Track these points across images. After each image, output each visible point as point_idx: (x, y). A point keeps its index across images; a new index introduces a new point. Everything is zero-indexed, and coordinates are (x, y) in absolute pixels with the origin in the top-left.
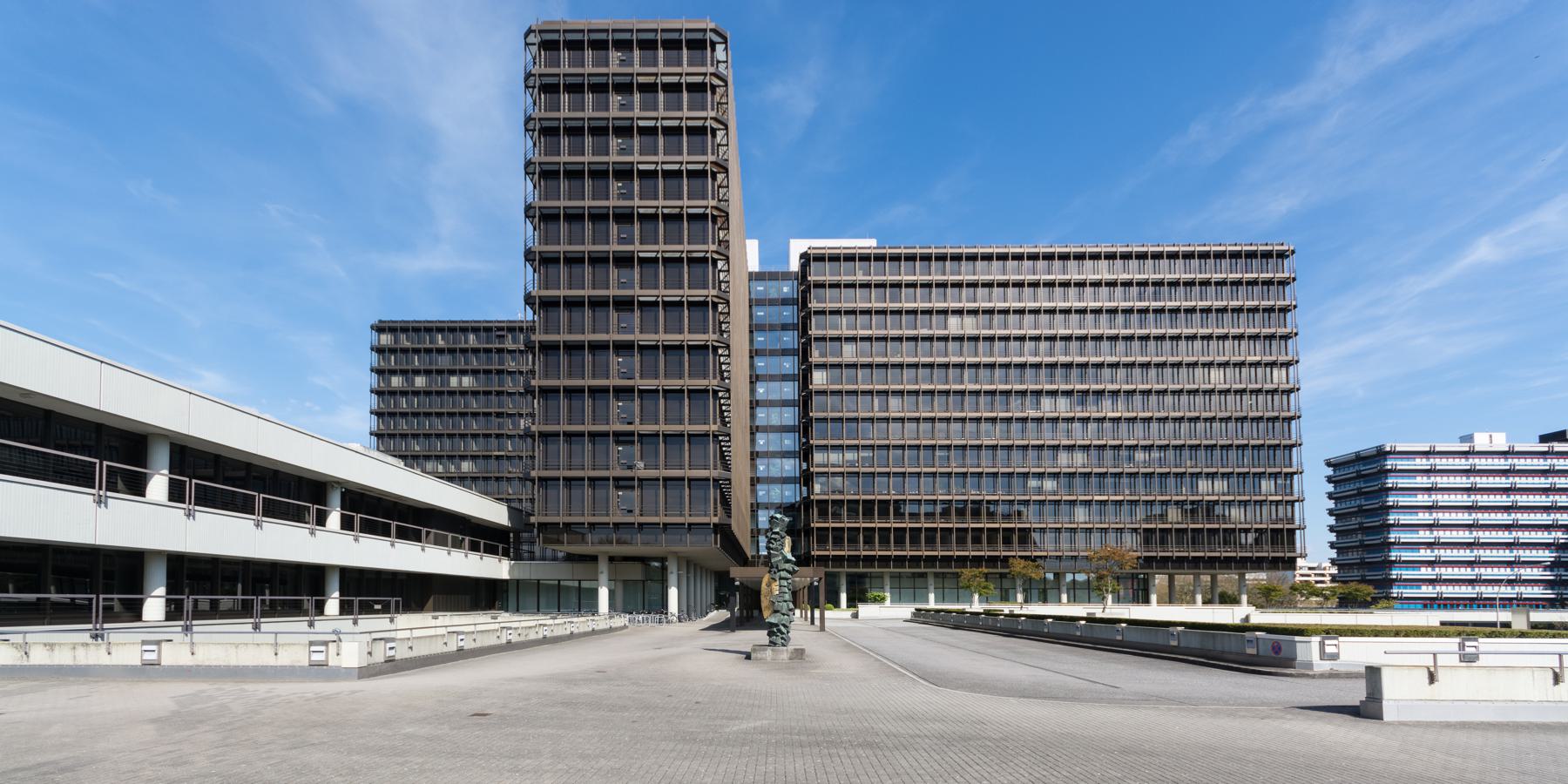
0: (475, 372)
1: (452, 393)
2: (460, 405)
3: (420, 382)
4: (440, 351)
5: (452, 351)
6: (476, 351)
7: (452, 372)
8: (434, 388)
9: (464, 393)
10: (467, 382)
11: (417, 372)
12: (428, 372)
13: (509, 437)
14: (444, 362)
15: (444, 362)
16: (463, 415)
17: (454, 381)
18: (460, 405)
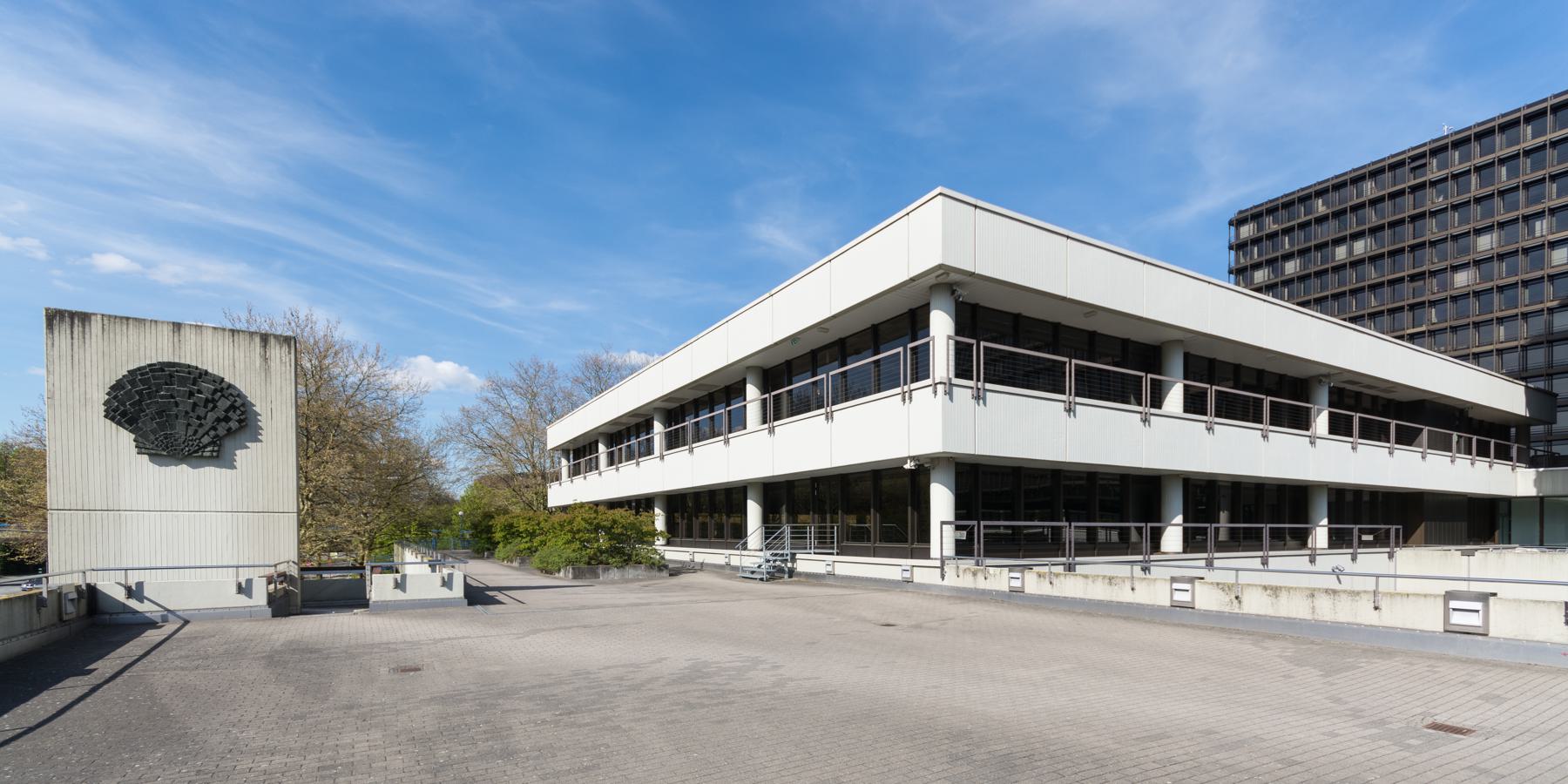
0: (1374, 231)
1: (1338, 268)
2: (1352, 279)
3: (1291, 268)
4: (1321, 220)
5: (1338, 215)
6: (1374, 202)
7: (1338, 242)
8: (1313, 269)
9: (1357, 263)
10: (1360, 247)
11: (1288, 257)
12: (1302, 253)
13: (1433, 303)
14: (1329, 231)
15: (1329, 231)
16: (1354, 292)
17: (1341, 253)
18: (1352, 279)
